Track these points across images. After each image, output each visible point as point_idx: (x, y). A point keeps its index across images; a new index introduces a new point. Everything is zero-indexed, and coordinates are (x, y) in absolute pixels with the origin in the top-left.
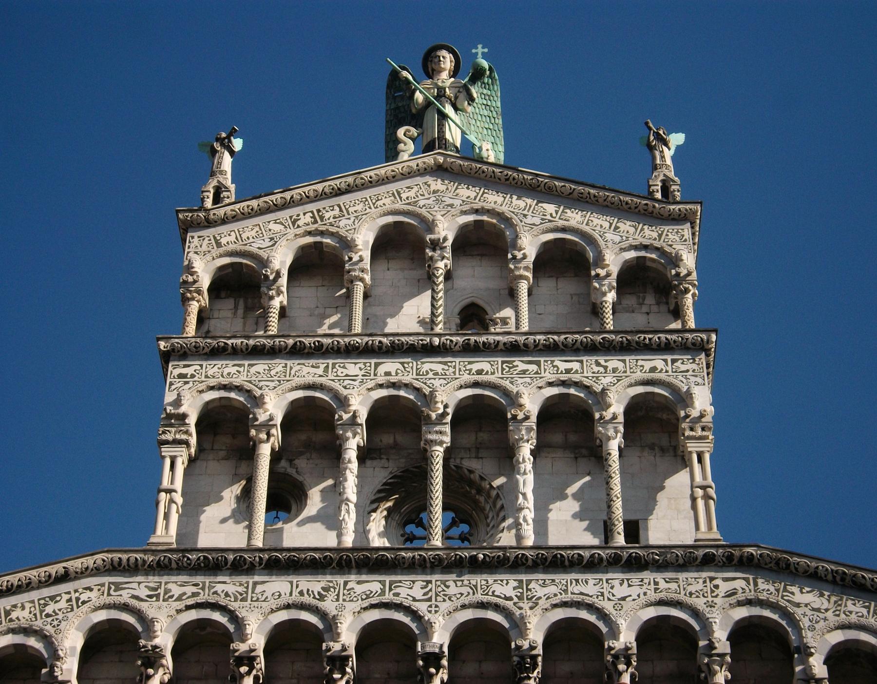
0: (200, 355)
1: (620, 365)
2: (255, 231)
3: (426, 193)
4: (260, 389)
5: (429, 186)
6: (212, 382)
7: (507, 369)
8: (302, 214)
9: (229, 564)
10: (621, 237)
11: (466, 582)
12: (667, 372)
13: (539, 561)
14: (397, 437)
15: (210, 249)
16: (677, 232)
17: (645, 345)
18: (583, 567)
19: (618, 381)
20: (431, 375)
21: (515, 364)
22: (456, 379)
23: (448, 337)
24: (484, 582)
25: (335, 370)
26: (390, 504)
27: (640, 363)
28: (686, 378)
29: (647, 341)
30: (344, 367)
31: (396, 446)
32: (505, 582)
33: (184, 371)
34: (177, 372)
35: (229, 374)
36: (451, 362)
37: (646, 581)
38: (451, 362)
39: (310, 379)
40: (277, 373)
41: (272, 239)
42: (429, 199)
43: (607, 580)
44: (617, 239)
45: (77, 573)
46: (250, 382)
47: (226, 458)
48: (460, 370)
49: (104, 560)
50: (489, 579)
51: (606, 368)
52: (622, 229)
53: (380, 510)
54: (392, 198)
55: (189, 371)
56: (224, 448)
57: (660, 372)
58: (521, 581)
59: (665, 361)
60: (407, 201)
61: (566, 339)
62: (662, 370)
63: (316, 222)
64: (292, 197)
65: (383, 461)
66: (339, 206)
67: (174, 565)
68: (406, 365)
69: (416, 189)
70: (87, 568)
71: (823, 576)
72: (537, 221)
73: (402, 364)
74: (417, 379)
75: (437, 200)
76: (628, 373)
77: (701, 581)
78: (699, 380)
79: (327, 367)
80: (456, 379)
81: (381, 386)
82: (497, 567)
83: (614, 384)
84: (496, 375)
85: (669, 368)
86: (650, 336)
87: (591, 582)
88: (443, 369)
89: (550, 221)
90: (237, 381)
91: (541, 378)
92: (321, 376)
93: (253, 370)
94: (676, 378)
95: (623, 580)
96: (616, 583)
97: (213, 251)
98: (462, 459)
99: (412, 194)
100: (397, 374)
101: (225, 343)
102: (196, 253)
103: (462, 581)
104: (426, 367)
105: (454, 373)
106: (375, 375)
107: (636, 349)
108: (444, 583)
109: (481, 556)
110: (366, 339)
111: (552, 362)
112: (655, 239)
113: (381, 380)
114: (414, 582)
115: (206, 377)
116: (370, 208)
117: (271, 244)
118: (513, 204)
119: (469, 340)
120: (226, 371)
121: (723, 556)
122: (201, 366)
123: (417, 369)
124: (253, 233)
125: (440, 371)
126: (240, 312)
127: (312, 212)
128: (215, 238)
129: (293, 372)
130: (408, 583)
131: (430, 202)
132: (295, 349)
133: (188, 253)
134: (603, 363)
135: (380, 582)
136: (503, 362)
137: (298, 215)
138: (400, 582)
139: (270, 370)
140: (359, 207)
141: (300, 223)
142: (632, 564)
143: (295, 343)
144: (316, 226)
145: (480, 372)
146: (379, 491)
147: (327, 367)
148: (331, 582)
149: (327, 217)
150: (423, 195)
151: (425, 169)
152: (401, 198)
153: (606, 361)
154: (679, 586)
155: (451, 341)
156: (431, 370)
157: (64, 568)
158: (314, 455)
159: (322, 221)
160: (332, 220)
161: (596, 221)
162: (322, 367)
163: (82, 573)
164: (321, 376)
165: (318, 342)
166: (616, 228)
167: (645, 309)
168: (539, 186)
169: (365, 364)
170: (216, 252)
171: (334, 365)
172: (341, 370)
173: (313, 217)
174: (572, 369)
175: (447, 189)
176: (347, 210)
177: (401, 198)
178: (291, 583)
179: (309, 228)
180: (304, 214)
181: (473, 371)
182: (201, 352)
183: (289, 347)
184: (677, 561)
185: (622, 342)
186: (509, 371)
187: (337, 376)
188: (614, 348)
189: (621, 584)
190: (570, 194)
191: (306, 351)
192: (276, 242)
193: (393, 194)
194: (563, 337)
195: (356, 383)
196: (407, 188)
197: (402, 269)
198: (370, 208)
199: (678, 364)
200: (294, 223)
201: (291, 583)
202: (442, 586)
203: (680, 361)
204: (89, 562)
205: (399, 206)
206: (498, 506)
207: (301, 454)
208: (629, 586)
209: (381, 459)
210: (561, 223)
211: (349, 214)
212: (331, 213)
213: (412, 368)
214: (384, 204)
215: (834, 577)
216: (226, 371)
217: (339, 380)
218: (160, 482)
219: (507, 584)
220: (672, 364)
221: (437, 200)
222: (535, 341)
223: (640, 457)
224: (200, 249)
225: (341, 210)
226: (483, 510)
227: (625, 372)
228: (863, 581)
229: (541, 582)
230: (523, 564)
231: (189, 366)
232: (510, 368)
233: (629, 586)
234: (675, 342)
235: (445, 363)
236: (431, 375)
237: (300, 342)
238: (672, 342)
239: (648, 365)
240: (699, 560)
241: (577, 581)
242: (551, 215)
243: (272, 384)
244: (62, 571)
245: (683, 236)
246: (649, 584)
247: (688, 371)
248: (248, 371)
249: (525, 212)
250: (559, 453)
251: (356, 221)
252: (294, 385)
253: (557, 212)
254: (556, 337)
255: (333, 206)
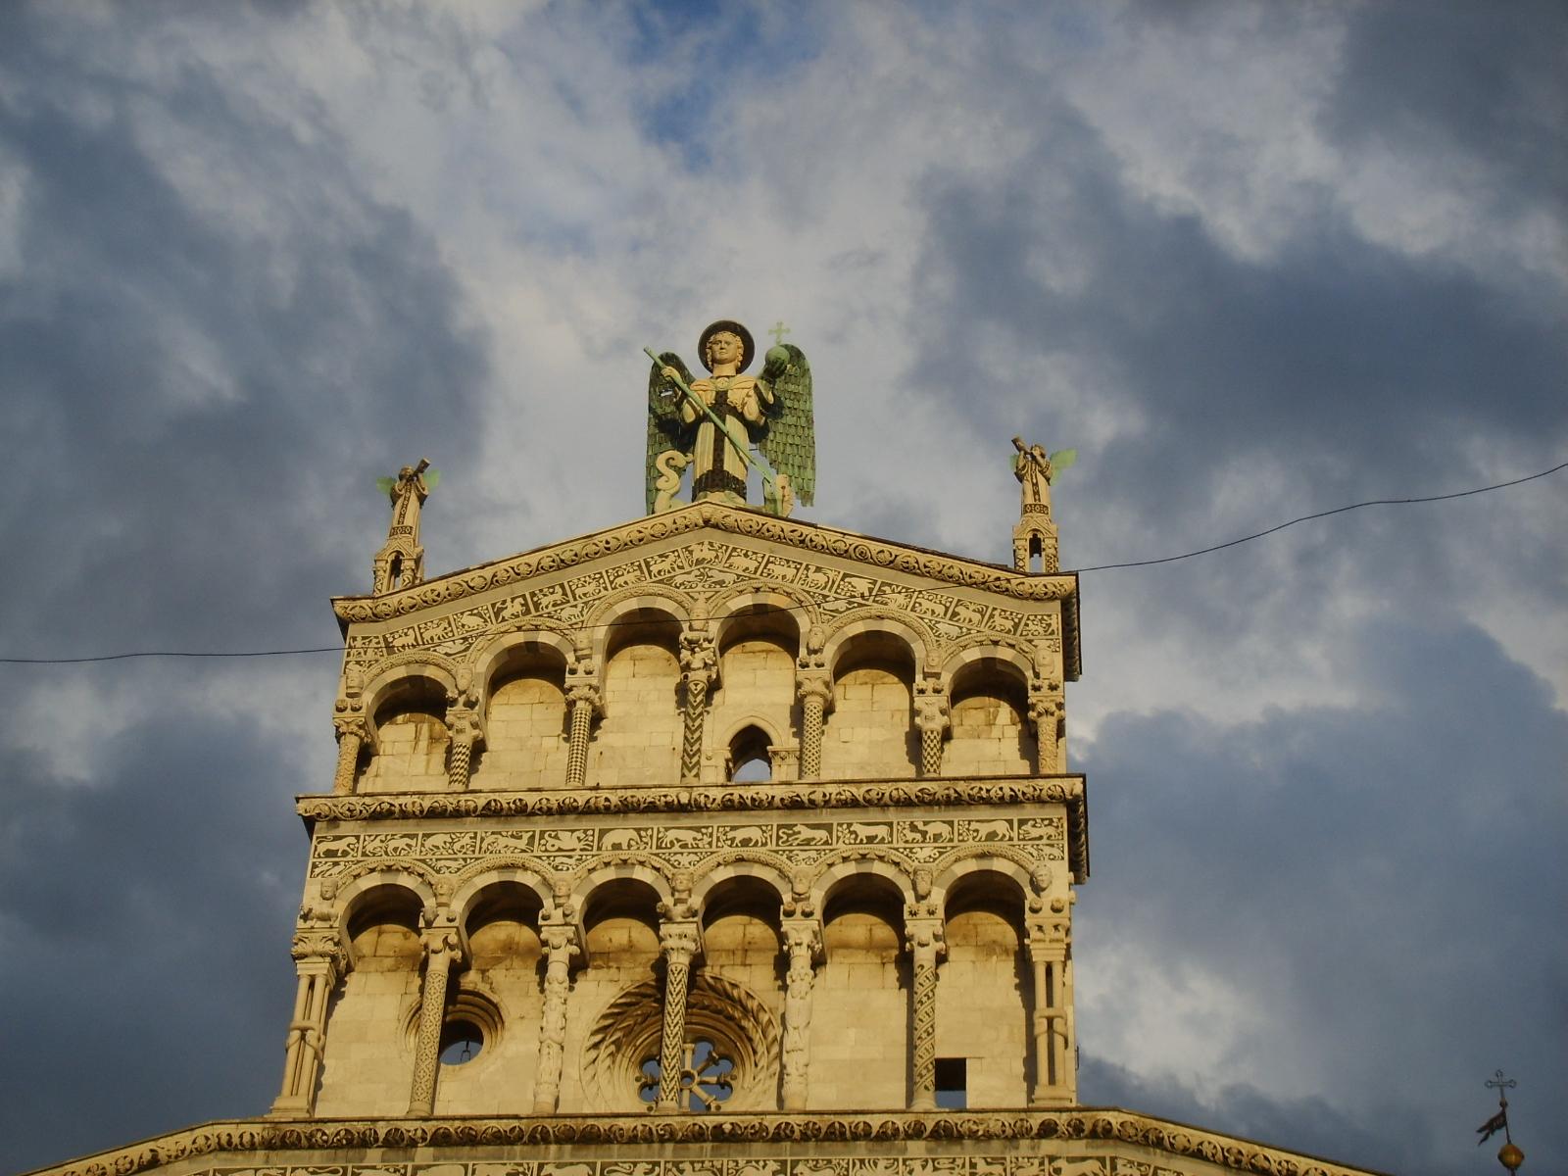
0: (357, 820)
1: (945, 829)
2: (442, 627)
3: (686, 566)
4: (438, 872)
5: (691, 552)
6: (371, 862)
7: (785, 837)
8: (509, 600)
9: (381, 1139)
10: (961, 628)
11: (707, 1164)
12: (1011, 839)
13: (809, 1132)
14: (632, 934)
15: (378, 657)
16: (1043, 619)
17: (981, 798)
18: (871, 1140)
19: (941, 853)
20: (676, 848)
21: (796, 829)
22: (712, 853)
23: (701, 790)
24: (732, 1164)
25: (543, 842)
26: (618, 1034)
27: (974, 826)
28: (1038, 850)
29: (984, 794)
30: (556, 837)
31: (630, 949)
32: (762, 1163)
33: (333, 846)
34: (323, 847)
35: (395, 849)
36: (707, 828)
37: (959, 1162)
38: (707, 828)
39: (507, 857)
40: (463, 847)
41: (465, 639)
42: (689, 573)
43: (904, 1161)
44: (954, 631)
45: (170, 1157)
46: (423, 861)
47: (394, 970)
48: (718, 838)
49: (207, 1138)
50: (740, 1159)
51: (924, 834)
52: (962, 617)
53: (606, 1043)
54: (638, 573)
55: (340, 845)
56: (392, 953)
57: (1001, 840)
58: (784, 1163)
59: (1010, 822)
60: (660, 578)
61: (868, 791)
62: (1004, 836)
63: (528, 612)
64: (494, 576)
65: (613, 971)
66: (562, 586)
67: (304, 1142)
68: (643, 833)
69: (672, 557)
70: (183, 1151)
71: (1209, 1155)
72: (842, 605)
73: (638, 830)
74: (657, 855)
75: (702, 574)
76: (956, 843)
77: (1036, 1162)
78: (1056, 852)
79: (533, 837)
80: (712, 853)
81: (607, 864)
82: (751, 1141)
83: (935, 859)
84: (769, 846)
85: (1015, 835)
86: (989, 787)
87: (882, 1164)
88: (695, 839)
89: (861, 605)
90: (405, 860)
91: (831, 850)
92: (523, 851)
93: (429, 843)
94: (1023, 849)
95: (926, 1161)
96: (917, 1165)
97: (383, 659)
98: (722, 966)
99: (666, 565)
100: (629, 846)
101: (392, 805)
102: (358, 663)
103: (703, 1162)
104: (672, 835)
105: (710, 844)
106: (599, 848)
107: (969, 804)
108: (676, 1164)
109: (727, 1127)
110: (589, 794)
111: (850, 825)
112: (1009, 631)
113: (607, 855)
114: (635, 1164)
115: (364, 854)
116: (606, 589)
117: (463, 647)
118: (809, 580)
119: (732, 794)
120: (392, 844)
121: (1069, 1125)
122: (357, 837)
123: (658, 839)
124: (439, 631)
125: (690, 841)
126: (424, 743)
127: (524, 596)
128: (385, 639)
129: (484, 846)
130: (626, 1166)
131: (691, 578)
132: (490, 810)
133: (347, 663)
134: (921, 827)
135: (588, 1164)
136: (780, 827)
137: (504, 602)
138: (616, 1164)
139: (452, 843)
140: (589, 589)
141: (506, 614)
142: (939, 1134)
143: (489, 803)
144: (528, 617)
145: (745, 842)
146: (605, 1017)
147: (533, 837)
148: (521, 1165)
149: (543, 605)
150: (682, 568)
151: (687, 527)
152: (650, 572)
153: (926, 823)
154: (1005, 1170)
155: (706, 796)
156: (678, 841)
157: (152, 1150)
158: (517, 963)
159: (537, 610)
160: (551, 609)
161: (926, 605)
162: (526, 836)
163: (177, 1157)
164: (523, 851)
165: (520, 800)
166: (955, 614)
167: (996, 732)
168: (846, 551)
169: (585, 831)
170: (385, 661)
171: (542, 833)
172: (552, 841)
173: (525, 605)
174: (876, 836)
175: (717, 557)
176: (573, 592)
177: (650, 572)
178: (466, 1167)
179: (517, 622)
180: (513, 600)
181: (737, 841)
182: (358, 816)
183: (480, 808)
184: (1004, 1132)
185: (948, 796)
186: (787, 841)
187: (546, 851)
188: (938, 803)
189: (924, 1167)
190: (891, 562)
191: (504, 813)
192: (471, 644)
193: (640, 566)
194: (865, 787)
195: (572, 861)
196: (660, 556)
197: (653, 675)
198: (606, 589)
199: (1027, 827)
200: (497, 615)
201: (466, 1167)
202: (674, 1169)
203: (1031, 823)
204: (185, 1140)
205: (648, 585)
206: (770, 1039)
207: (498, 961)
208: (935, 1169)
209: (609, 967)
210: (876, 609)
211: (575, 599)
212: (551, 598)
213: (651, 837)
214: (626, 583)
215: (1225, 1158)
216: (392, 844)
217: (548, 857)
218: (291, 1017)
219: (764, 1167)
220: (1019, 828)
221: (702, 574)
222: (825, 795)
223: (974, 962)
224: (364, 657)
225: (565, 594)
226: (750, 1040)
227: (951, 840)
228: (1266, 1164)
229: (811, 1164)
230: (788, 1138)
231: (340, 838)
232: (789, 835)
233: (935, 1169)
234: (1024, 794)
235: (698, 829)
236: (676, 848)
237: (495, 800)
238: (1020, 794)
239: (984, 829)
240: (1035, 1131)
241: (862, 1162)
242: (862, 596)
243: (454, 865)
244: (147, 1156)
245: (1049, 625)
246: (964, 1166)
247: (1041, 838)
248: (423, 845)
249: (825, 592)
250: (860, 957)
251: (586, 611)
252: (484, 865)
253: (871, 590)
254: (854, 790)
255: (553, 587)
